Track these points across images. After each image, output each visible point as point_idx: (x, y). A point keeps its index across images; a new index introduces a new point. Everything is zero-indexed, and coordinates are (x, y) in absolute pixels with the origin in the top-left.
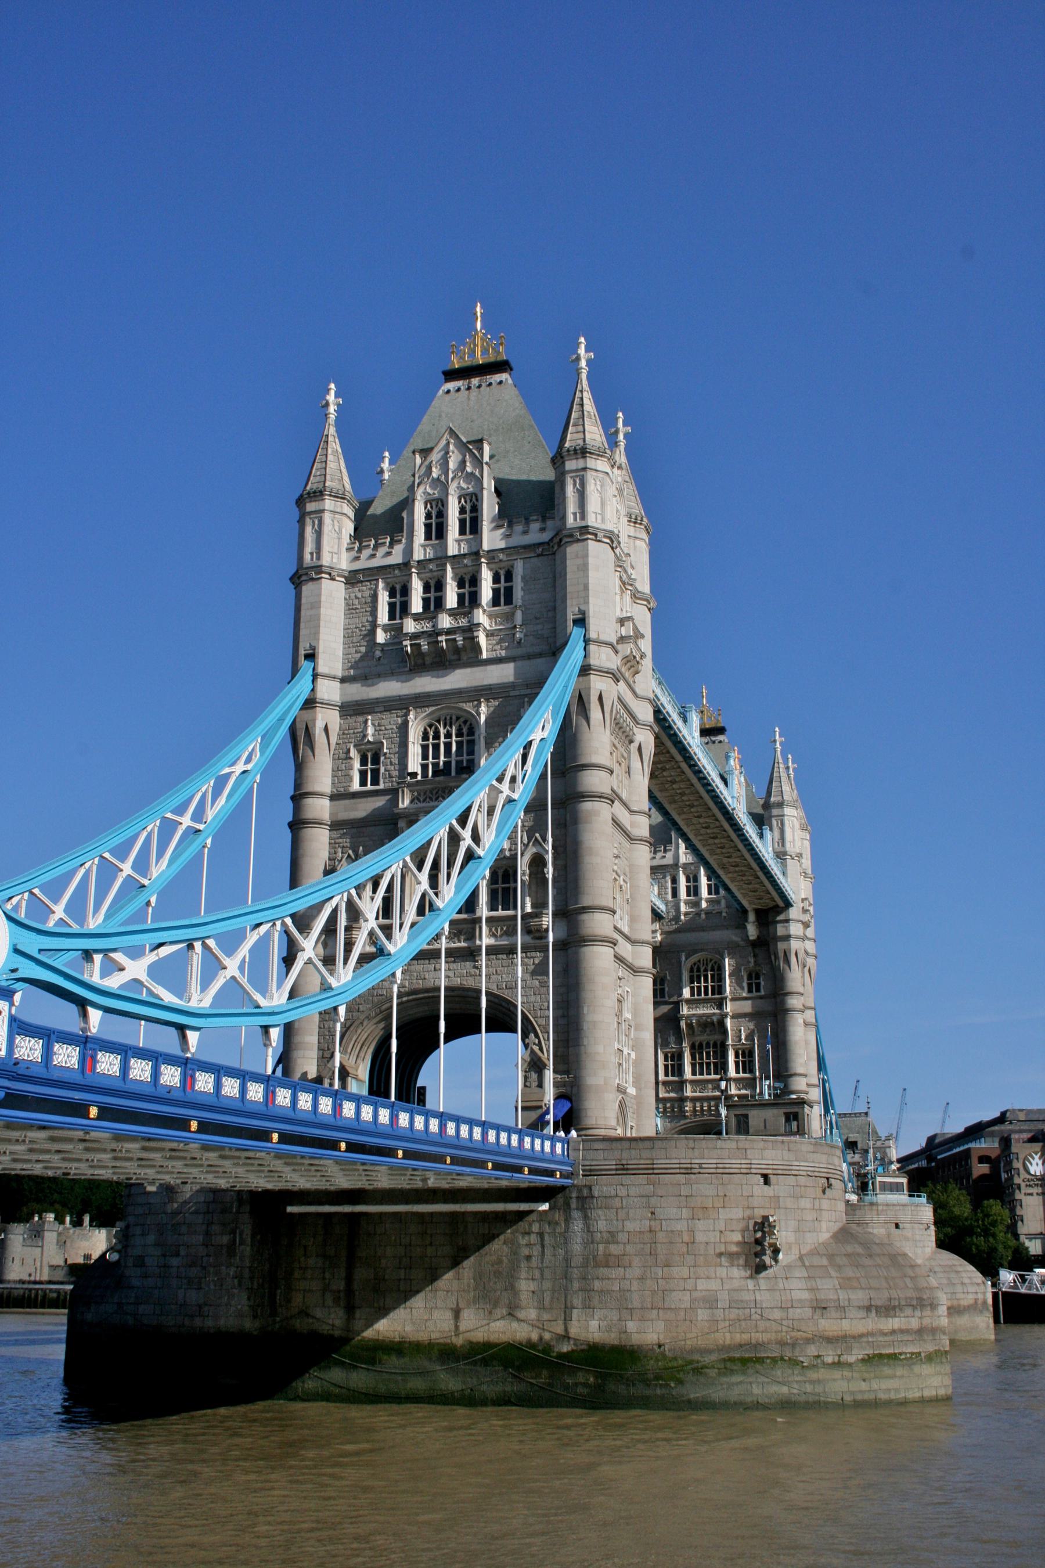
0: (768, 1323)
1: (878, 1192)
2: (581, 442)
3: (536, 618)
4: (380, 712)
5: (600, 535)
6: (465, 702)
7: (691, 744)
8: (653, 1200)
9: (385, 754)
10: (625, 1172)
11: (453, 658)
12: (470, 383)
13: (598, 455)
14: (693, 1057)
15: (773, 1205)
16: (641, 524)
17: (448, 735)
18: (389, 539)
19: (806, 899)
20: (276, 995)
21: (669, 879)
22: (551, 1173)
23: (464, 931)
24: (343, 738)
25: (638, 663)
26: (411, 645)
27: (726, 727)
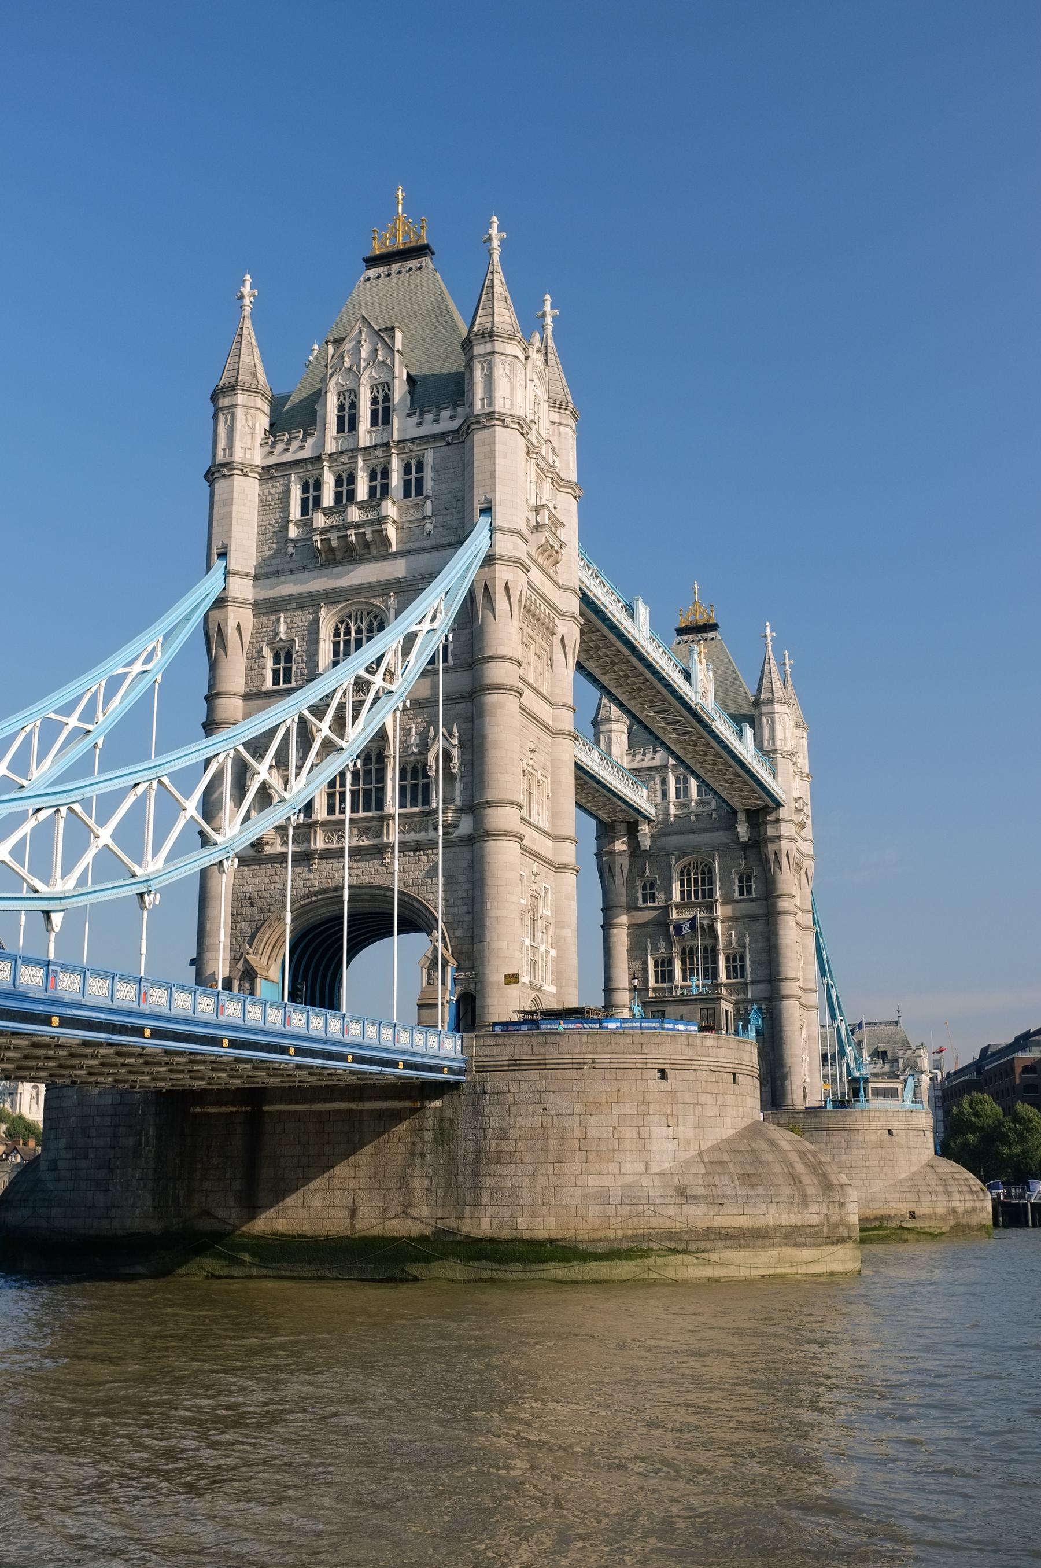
0: (661, 1220)
1: (870, 1097)
2: (489, 325)
3: (446, 509)
6: (376, 597)
7: (637, 637)
9: (297, 652)
10: (517, 1068)
11: (363, 552)
12: (390, 269)
14: (684, 963)
15: (670, 1100)
16: (566, 409)
18: (302, 432)
19: (800, 798)
20: (59, 882)
21: (658, 780)
22: (438, 1069)
25: (557, 552)
26: (321, 540)
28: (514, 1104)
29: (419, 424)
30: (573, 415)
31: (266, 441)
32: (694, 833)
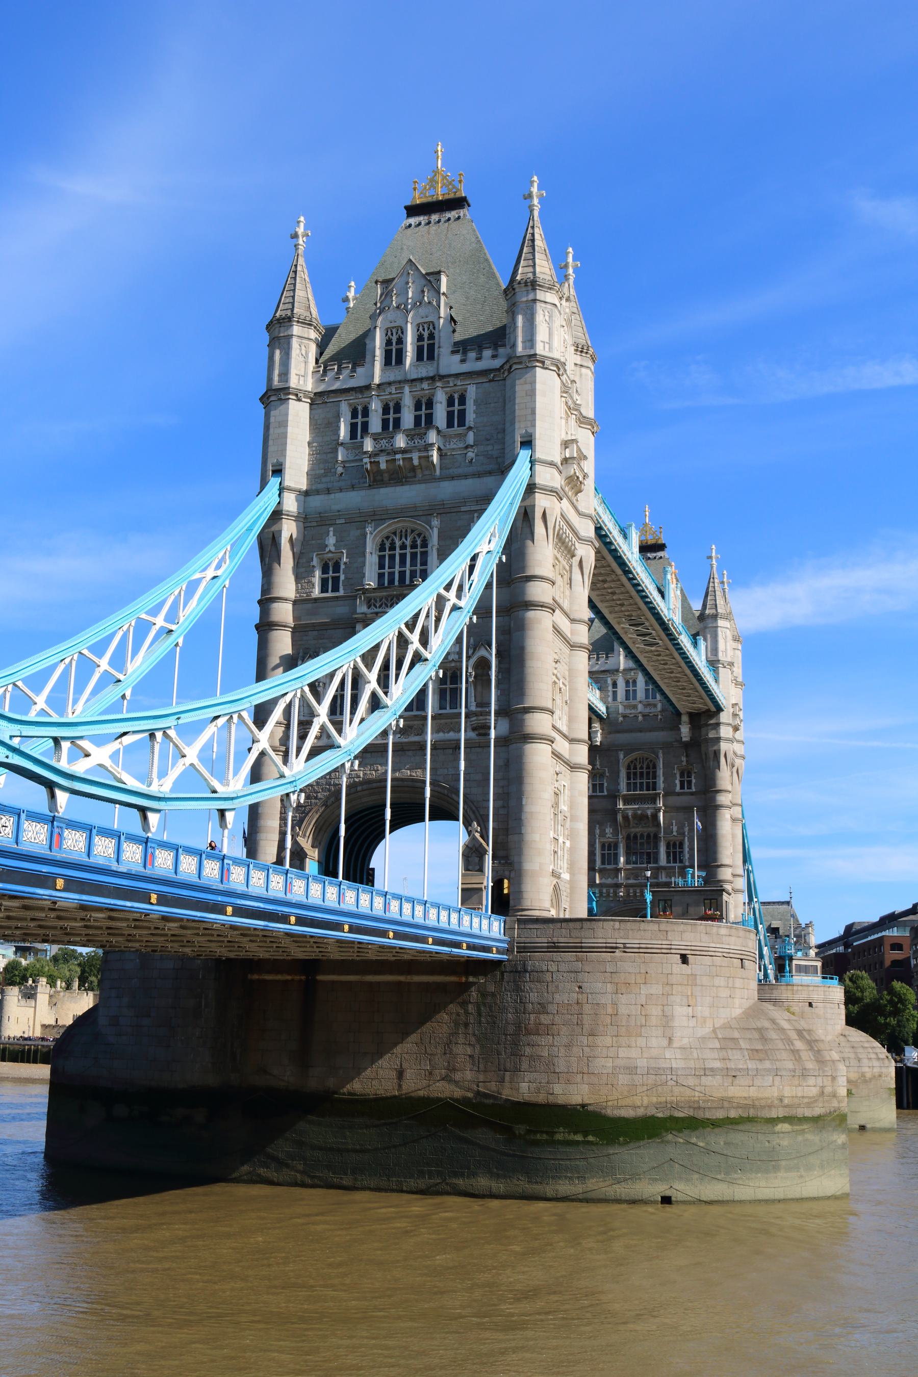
0: (682, 1089)
1: (794, 974)
2: (530, 275)
5: (547, 362)
7: (630, 559)
9: (345, 563)
11: (409, 475)
15: (690, 982)
16: (587, 353)
17: (403, 547)
19: (736, 704)
20: (232, 782)
22: (487, 949)
25: (581, 483)
26: (371, 462)
27: (667, 545)
29: (463, 361)
30: (592, 358)
32: (641, 732)
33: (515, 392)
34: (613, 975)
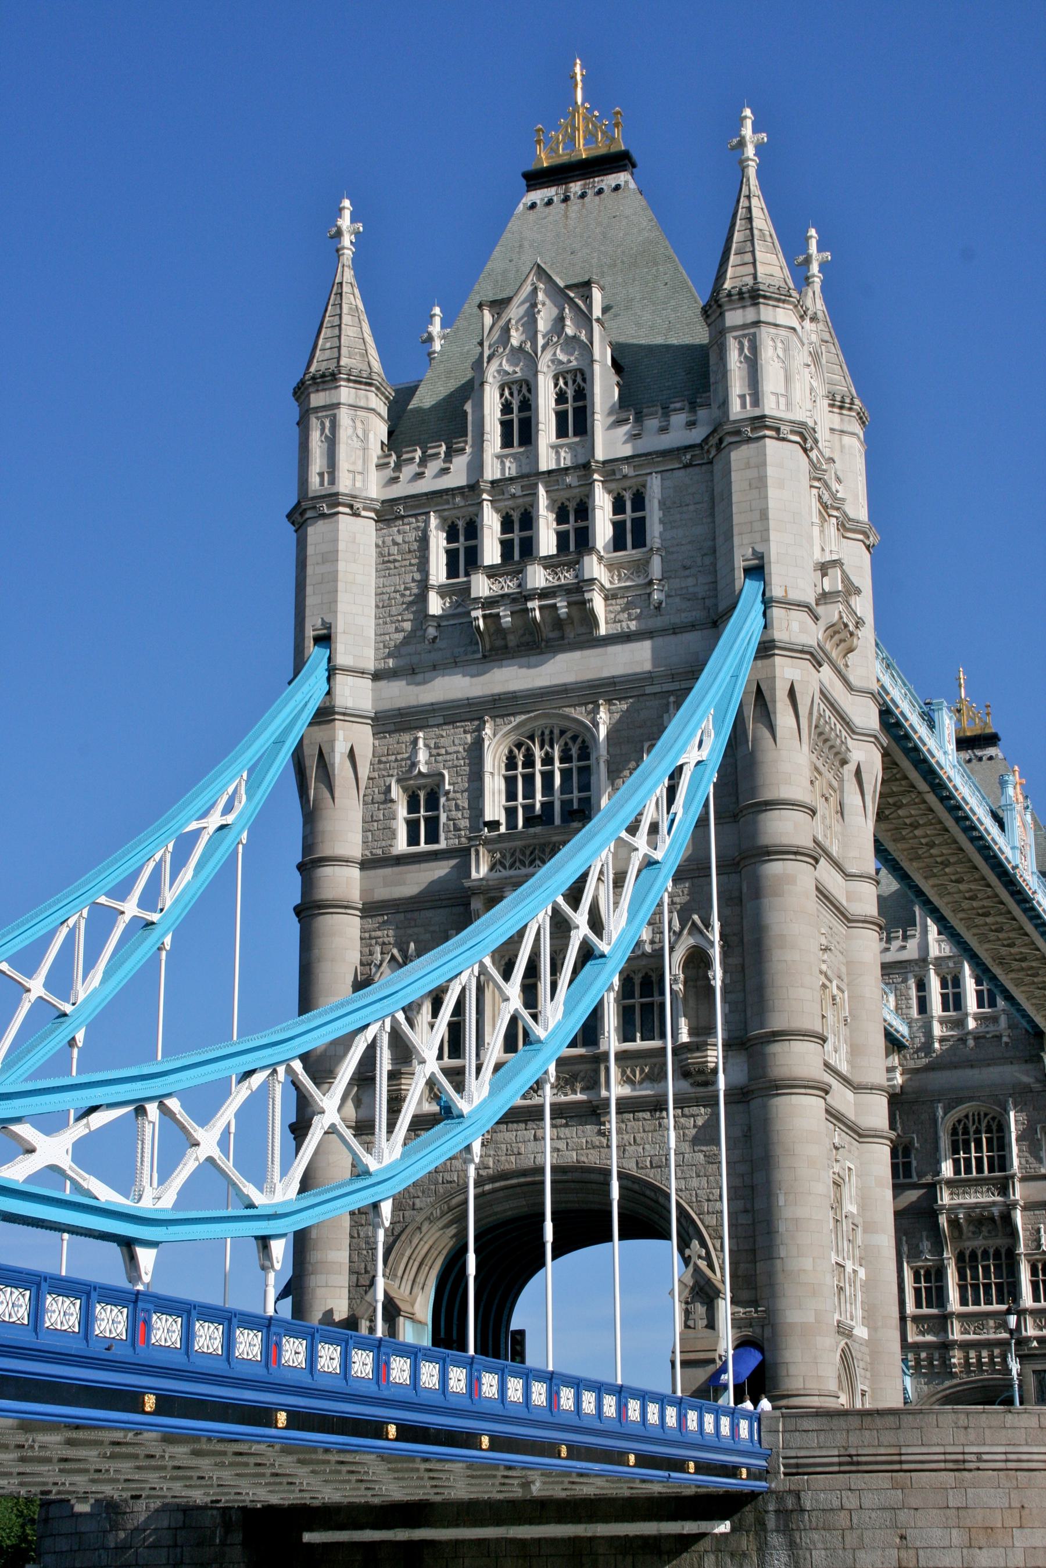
2: (749, 280)
3: (685, 568)
4: (438, 726)
5: (785, 429)
6: (574, 706)
7: (942, 762)
8: (903, 1516)
9: (447, 793)
10: (853, 1468)
11: (551, 635)
12: (567, 190)
13: (779, 300)
14: (962, 1276)
16: (850, 409)
17: (548, 760)
18: (444, 448)
20: (279, 1186)
21: (912, 983)
22: (732, 1471)
23: (582, 1074)
24: (380, 769)
25: (852, 634)
26: (484, 617)
27: (1000, 735)
28: (852, 1528)
30: (861, 418)
31: (386, 460)
33: (729, 483)
34: (962, 1513)
